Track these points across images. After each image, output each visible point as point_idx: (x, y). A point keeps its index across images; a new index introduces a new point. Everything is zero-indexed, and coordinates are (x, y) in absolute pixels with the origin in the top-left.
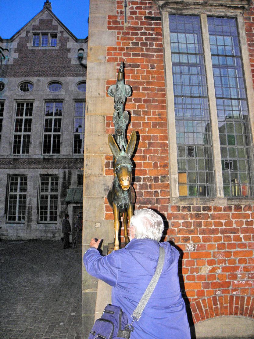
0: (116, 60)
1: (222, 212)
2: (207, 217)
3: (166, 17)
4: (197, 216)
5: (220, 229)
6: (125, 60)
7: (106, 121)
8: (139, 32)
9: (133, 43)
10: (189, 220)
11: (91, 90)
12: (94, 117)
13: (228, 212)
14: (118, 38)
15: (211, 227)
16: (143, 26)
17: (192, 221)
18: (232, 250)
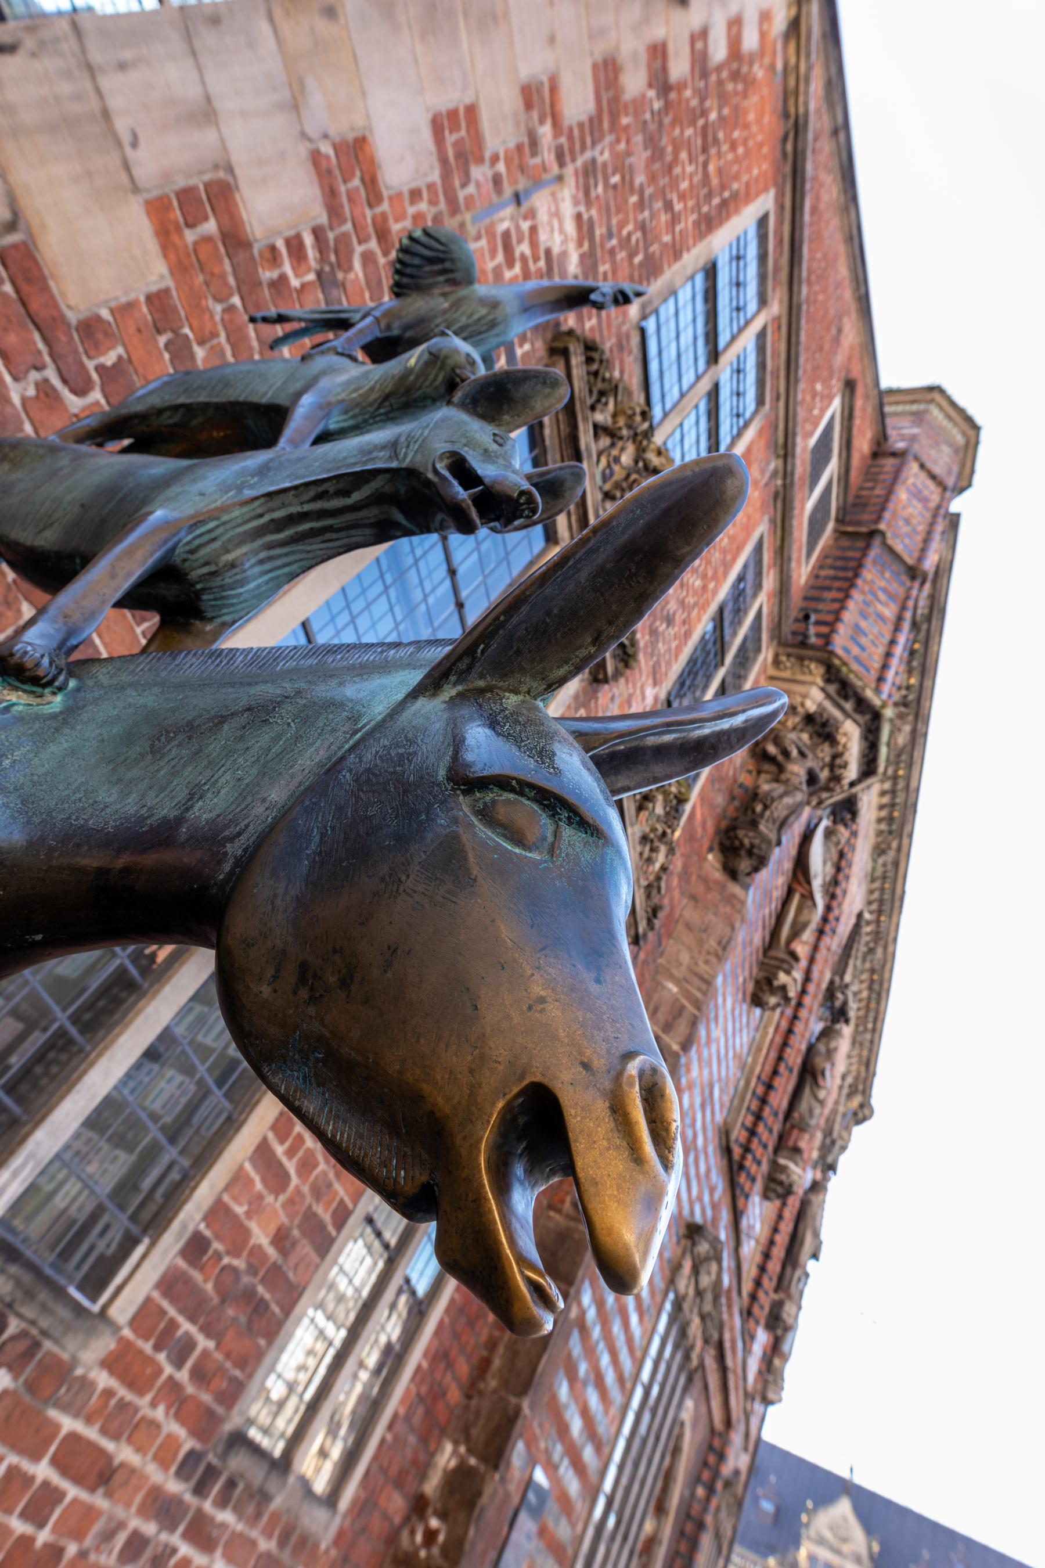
0: (334, 211)
6: (351, 276)
14: (415, 195)
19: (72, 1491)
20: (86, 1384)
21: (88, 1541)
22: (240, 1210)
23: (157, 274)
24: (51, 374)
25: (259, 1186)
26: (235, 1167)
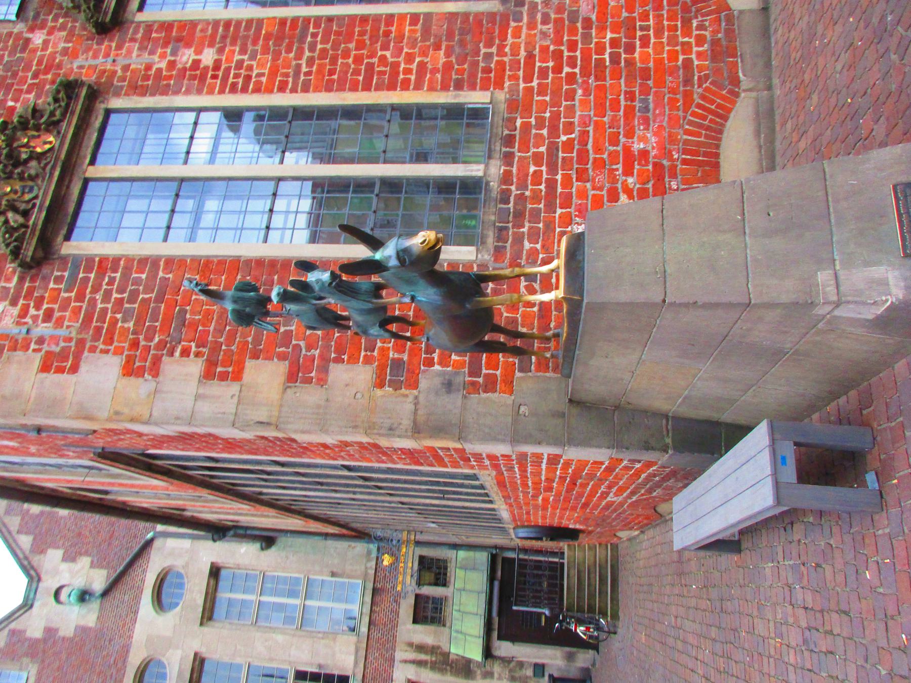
0: (157, 361)
1: (514, 170)
2: (521, 198)
3: (77, 248)
4: (519, 215)
5: (547, 174)
7: (297, 384)
8: (100, 306)
9: (125, 320)
10: (525, 230)
11: (220, 415)
12: (285, 409)
13: (516, 159)
15: (541, 191)
16: (88, 297)
17: (527, 225)
18: (592, 156)
19: (538, 64)
20: (510, 91)
21: (548, 43)
22: (439, 76)
23: (250, 364)
24: (304, 352)
25: (428, 76)
26: (429, 93)
